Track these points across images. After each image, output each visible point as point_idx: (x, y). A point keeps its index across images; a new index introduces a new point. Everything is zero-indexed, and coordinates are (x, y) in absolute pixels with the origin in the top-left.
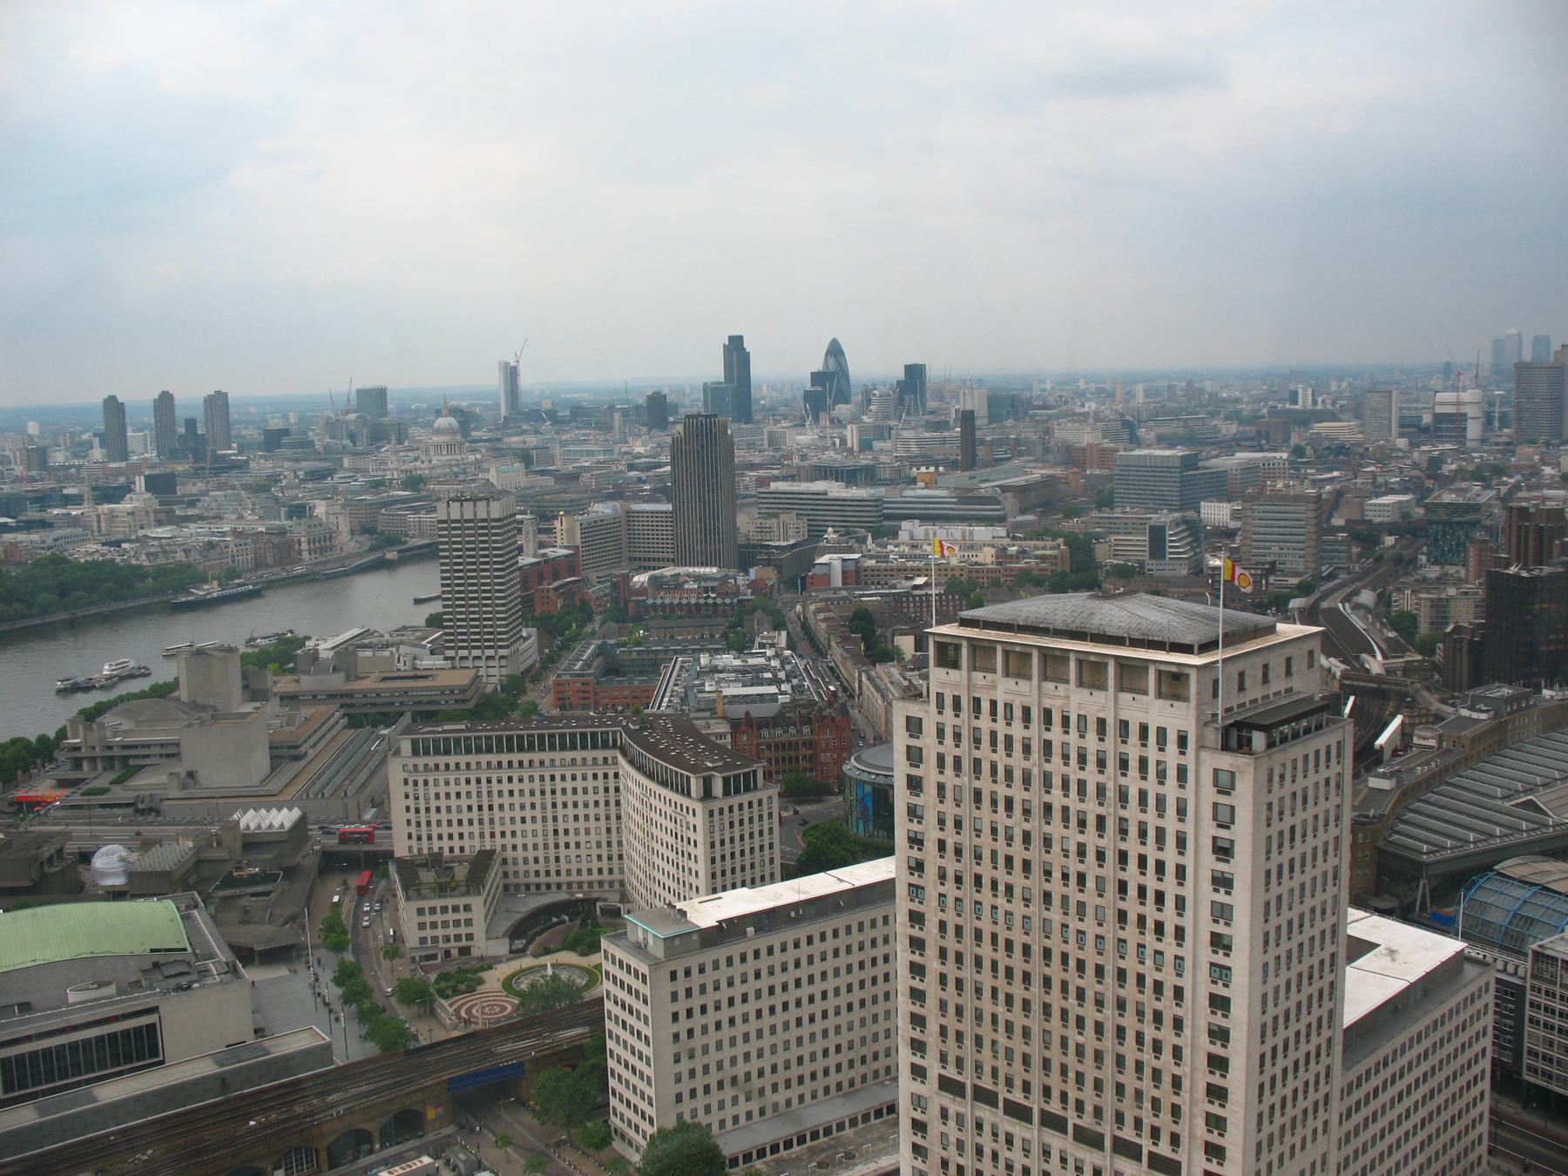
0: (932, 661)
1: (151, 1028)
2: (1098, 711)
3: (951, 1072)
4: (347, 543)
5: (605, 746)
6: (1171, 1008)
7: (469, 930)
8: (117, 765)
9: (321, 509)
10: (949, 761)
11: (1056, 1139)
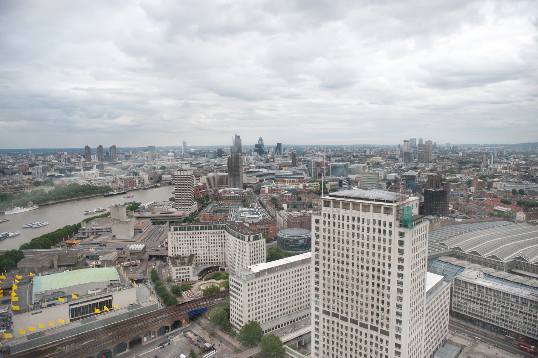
0: (323, 205)
1: (110, 300)
3: (326, 309)
4: (147, 181)
5: (222, 229)
7: (188, 274)
8: (95, 234)
9: (141, 173)
10: (327, 230)
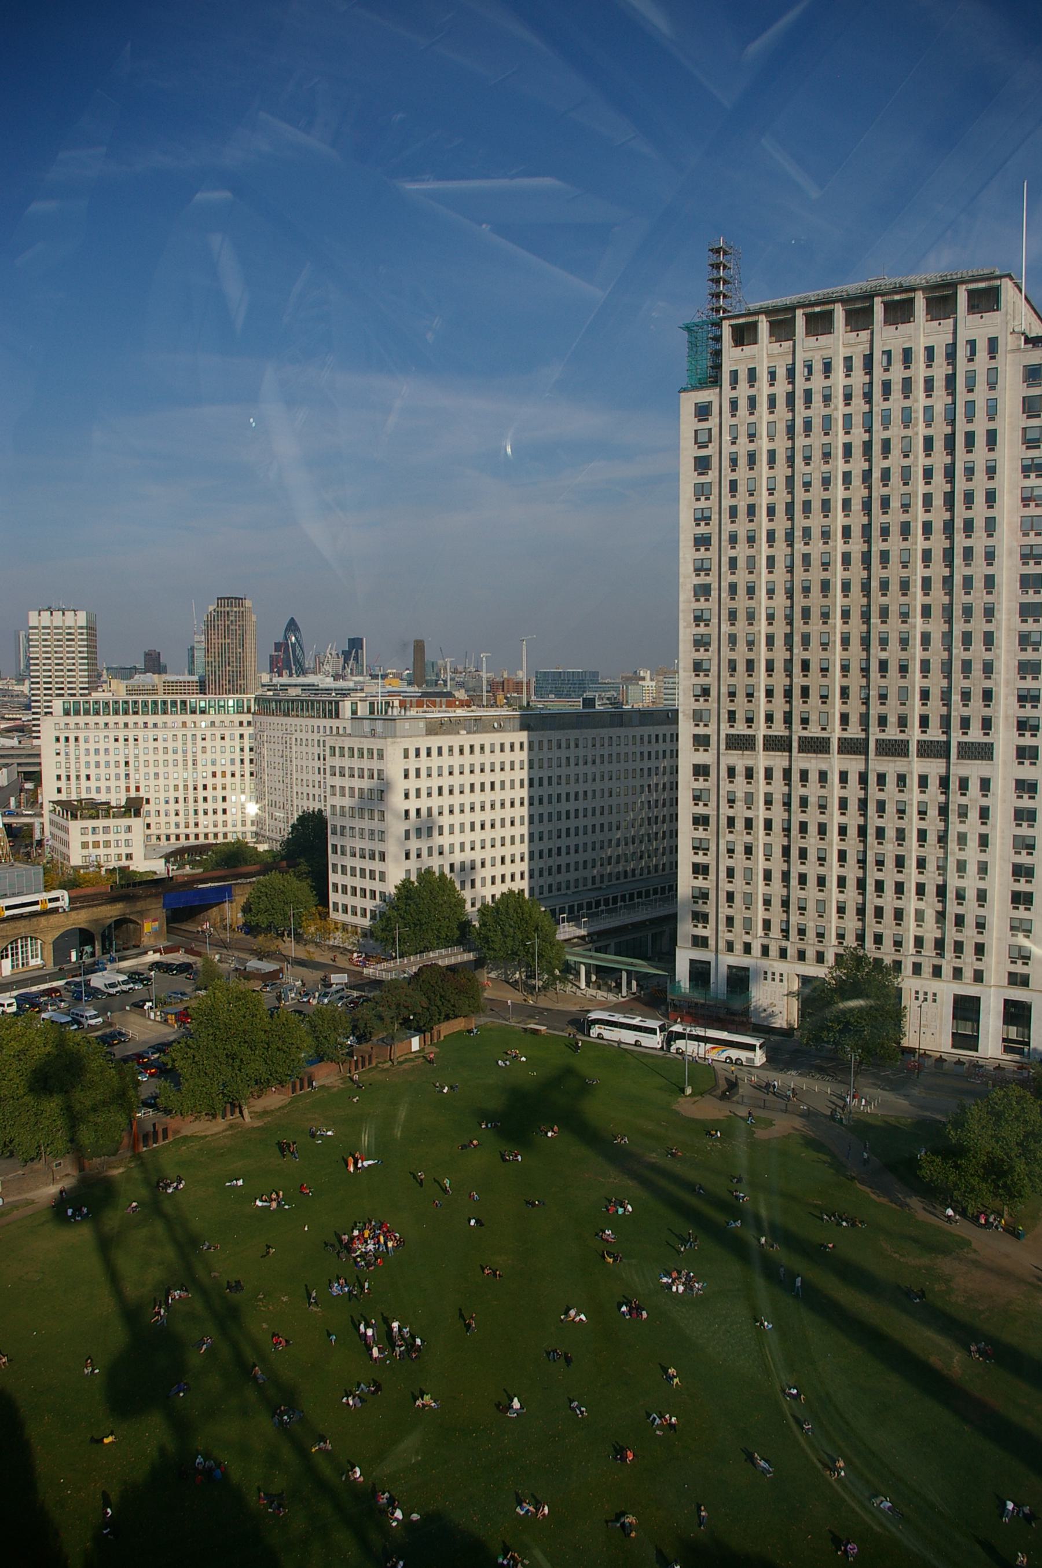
2: (904, 343)
3: (741, 728)
6: (982, 598)
11: (854, 762)
